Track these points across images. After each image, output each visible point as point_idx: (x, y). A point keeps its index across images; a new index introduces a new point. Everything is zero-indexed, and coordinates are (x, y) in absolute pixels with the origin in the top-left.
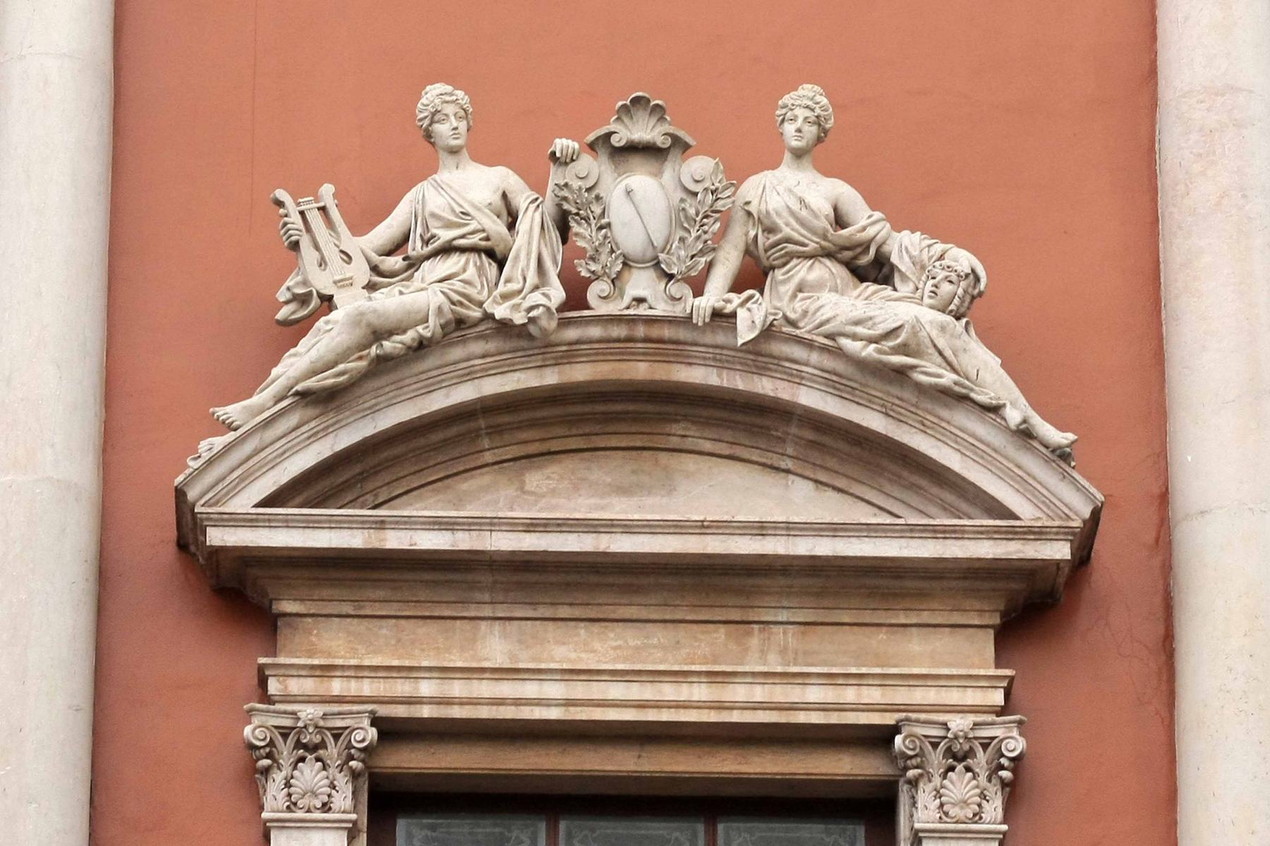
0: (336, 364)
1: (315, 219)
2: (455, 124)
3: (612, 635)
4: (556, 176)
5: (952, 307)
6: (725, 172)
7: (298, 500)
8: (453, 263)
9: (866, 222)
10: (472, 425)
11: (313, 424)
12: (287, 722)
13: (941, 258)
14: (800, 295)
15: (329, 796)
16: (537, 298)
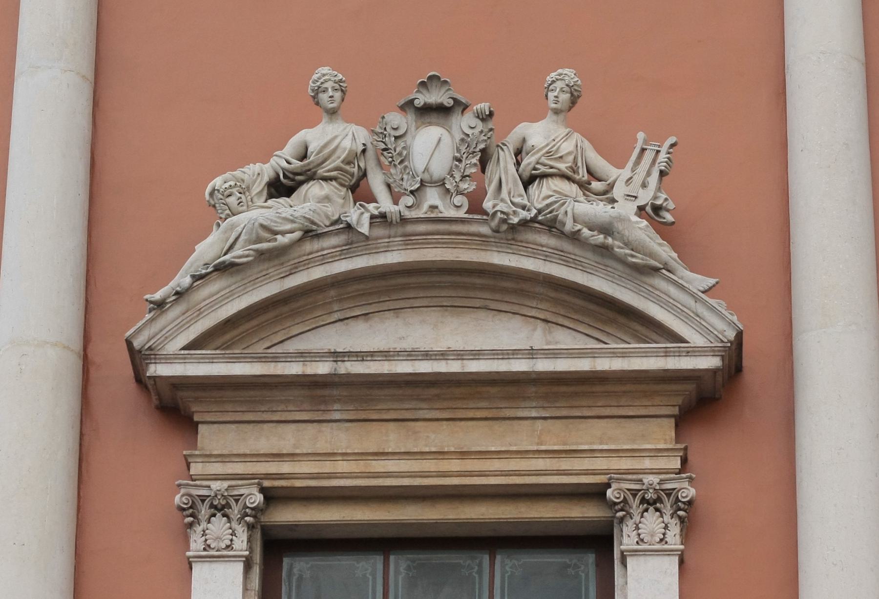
15: (231, 540)
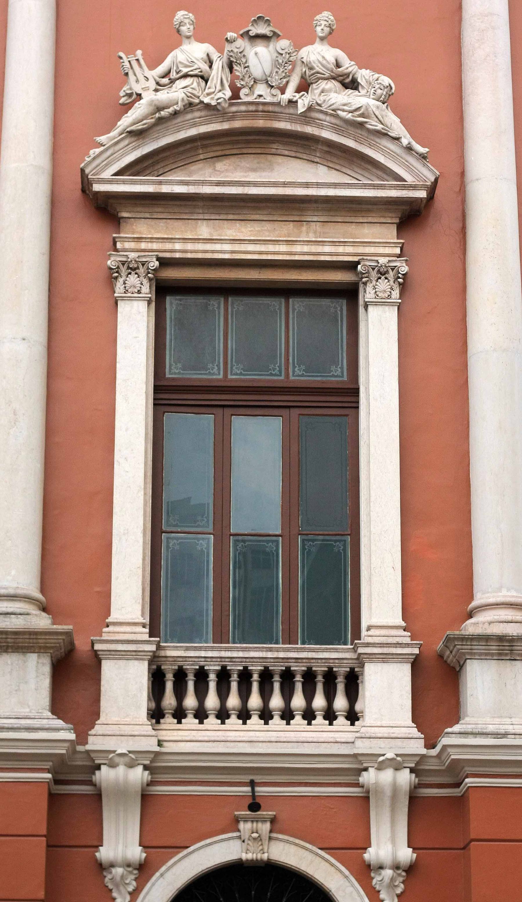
0: (142, 120)
1: (135, 64)
2: (189, 27)
3: (249, 226)
4: (228, 47)
5: (381, 99)
6: (293, 46)
7: (128, 173)
8: (188, 81)
9: (348, 65)
10: (196, 144)
11: (134, 144)
12: (124, 259)
13: (377, 80)
14: (323, 94)
15: (140, 287)
16: (220, 95)
